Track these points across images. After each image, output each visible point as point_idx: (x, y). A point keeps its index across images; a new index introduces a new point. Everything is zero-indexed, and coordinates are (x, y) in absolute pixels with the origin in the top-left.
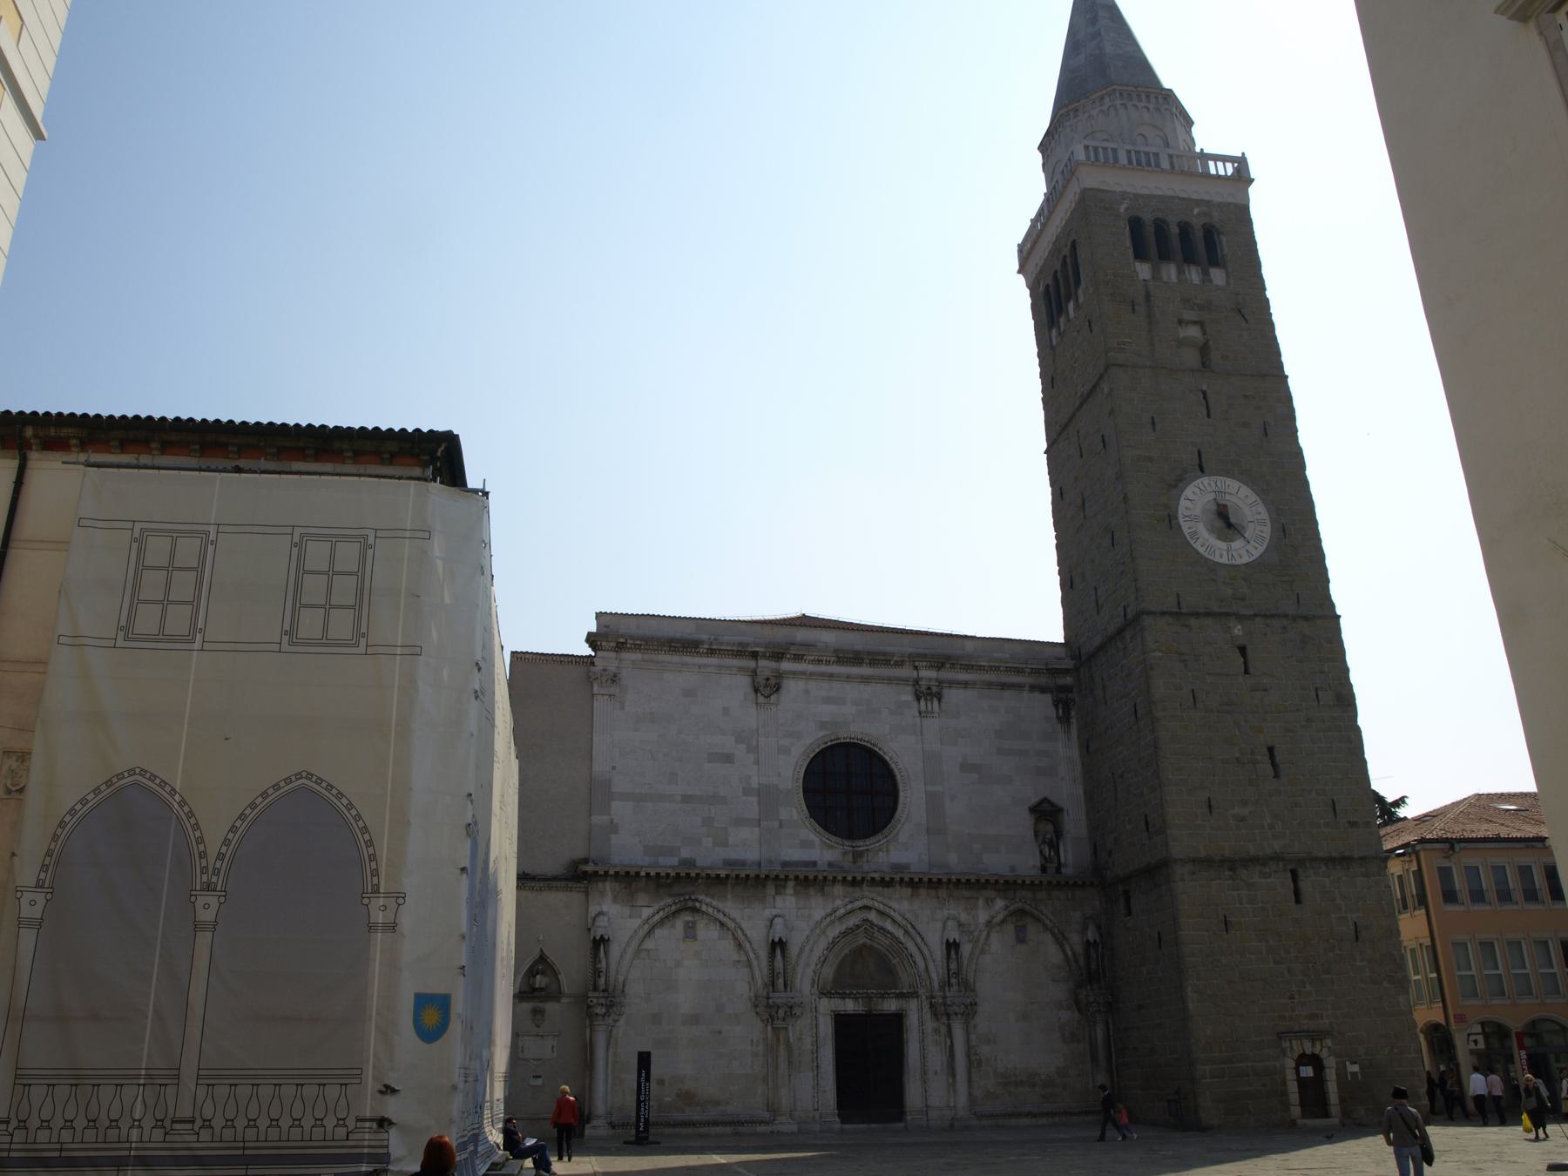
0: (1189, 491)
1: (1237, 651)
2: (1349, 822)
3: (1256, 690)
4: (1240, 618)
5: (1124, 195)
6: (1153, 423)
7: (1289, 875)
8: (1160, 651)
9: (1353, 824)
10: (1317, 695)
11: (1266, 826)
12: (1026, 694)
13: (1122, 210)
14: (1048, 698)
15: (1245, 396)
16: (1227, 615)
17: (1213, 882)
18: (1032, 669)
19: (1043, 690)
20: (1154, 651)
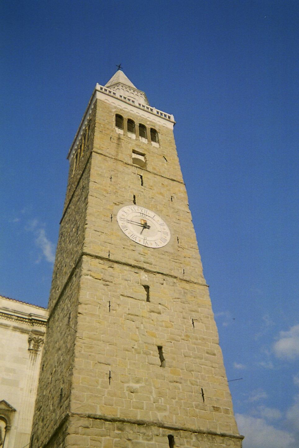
0: (126, 209)
1: (143, 287)
2: (214, 407)
3: (153, 312)
4: (146, 271)
5: (116, 108)
6: (111, 178)
7: (167, 440)
8: (91, 276)
9: (216, 409)
10: (193, 323)
11: (152, 399)
12: (9, 332)
13: (114, 110)
14: (26, 337)
15: (163, 184)
16: (140, 268)
17: (103, 438)
18: (18, 317)
19: (23, 331)
20: (87, 275)
